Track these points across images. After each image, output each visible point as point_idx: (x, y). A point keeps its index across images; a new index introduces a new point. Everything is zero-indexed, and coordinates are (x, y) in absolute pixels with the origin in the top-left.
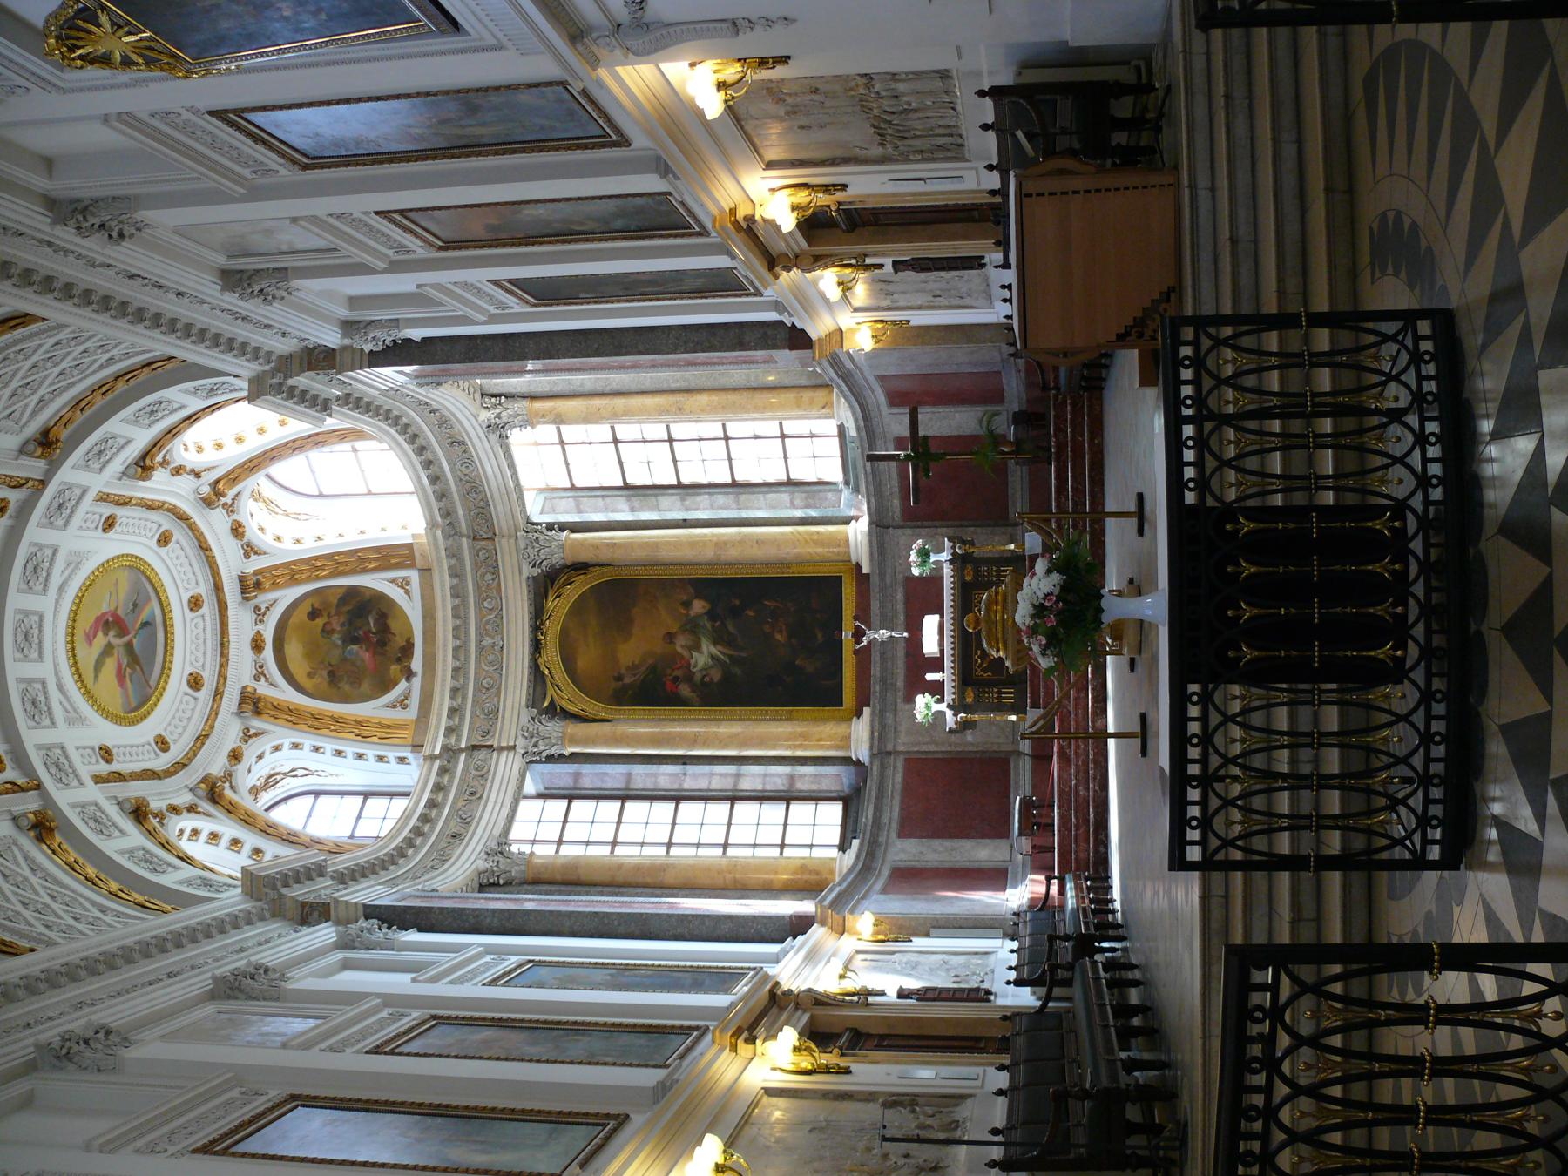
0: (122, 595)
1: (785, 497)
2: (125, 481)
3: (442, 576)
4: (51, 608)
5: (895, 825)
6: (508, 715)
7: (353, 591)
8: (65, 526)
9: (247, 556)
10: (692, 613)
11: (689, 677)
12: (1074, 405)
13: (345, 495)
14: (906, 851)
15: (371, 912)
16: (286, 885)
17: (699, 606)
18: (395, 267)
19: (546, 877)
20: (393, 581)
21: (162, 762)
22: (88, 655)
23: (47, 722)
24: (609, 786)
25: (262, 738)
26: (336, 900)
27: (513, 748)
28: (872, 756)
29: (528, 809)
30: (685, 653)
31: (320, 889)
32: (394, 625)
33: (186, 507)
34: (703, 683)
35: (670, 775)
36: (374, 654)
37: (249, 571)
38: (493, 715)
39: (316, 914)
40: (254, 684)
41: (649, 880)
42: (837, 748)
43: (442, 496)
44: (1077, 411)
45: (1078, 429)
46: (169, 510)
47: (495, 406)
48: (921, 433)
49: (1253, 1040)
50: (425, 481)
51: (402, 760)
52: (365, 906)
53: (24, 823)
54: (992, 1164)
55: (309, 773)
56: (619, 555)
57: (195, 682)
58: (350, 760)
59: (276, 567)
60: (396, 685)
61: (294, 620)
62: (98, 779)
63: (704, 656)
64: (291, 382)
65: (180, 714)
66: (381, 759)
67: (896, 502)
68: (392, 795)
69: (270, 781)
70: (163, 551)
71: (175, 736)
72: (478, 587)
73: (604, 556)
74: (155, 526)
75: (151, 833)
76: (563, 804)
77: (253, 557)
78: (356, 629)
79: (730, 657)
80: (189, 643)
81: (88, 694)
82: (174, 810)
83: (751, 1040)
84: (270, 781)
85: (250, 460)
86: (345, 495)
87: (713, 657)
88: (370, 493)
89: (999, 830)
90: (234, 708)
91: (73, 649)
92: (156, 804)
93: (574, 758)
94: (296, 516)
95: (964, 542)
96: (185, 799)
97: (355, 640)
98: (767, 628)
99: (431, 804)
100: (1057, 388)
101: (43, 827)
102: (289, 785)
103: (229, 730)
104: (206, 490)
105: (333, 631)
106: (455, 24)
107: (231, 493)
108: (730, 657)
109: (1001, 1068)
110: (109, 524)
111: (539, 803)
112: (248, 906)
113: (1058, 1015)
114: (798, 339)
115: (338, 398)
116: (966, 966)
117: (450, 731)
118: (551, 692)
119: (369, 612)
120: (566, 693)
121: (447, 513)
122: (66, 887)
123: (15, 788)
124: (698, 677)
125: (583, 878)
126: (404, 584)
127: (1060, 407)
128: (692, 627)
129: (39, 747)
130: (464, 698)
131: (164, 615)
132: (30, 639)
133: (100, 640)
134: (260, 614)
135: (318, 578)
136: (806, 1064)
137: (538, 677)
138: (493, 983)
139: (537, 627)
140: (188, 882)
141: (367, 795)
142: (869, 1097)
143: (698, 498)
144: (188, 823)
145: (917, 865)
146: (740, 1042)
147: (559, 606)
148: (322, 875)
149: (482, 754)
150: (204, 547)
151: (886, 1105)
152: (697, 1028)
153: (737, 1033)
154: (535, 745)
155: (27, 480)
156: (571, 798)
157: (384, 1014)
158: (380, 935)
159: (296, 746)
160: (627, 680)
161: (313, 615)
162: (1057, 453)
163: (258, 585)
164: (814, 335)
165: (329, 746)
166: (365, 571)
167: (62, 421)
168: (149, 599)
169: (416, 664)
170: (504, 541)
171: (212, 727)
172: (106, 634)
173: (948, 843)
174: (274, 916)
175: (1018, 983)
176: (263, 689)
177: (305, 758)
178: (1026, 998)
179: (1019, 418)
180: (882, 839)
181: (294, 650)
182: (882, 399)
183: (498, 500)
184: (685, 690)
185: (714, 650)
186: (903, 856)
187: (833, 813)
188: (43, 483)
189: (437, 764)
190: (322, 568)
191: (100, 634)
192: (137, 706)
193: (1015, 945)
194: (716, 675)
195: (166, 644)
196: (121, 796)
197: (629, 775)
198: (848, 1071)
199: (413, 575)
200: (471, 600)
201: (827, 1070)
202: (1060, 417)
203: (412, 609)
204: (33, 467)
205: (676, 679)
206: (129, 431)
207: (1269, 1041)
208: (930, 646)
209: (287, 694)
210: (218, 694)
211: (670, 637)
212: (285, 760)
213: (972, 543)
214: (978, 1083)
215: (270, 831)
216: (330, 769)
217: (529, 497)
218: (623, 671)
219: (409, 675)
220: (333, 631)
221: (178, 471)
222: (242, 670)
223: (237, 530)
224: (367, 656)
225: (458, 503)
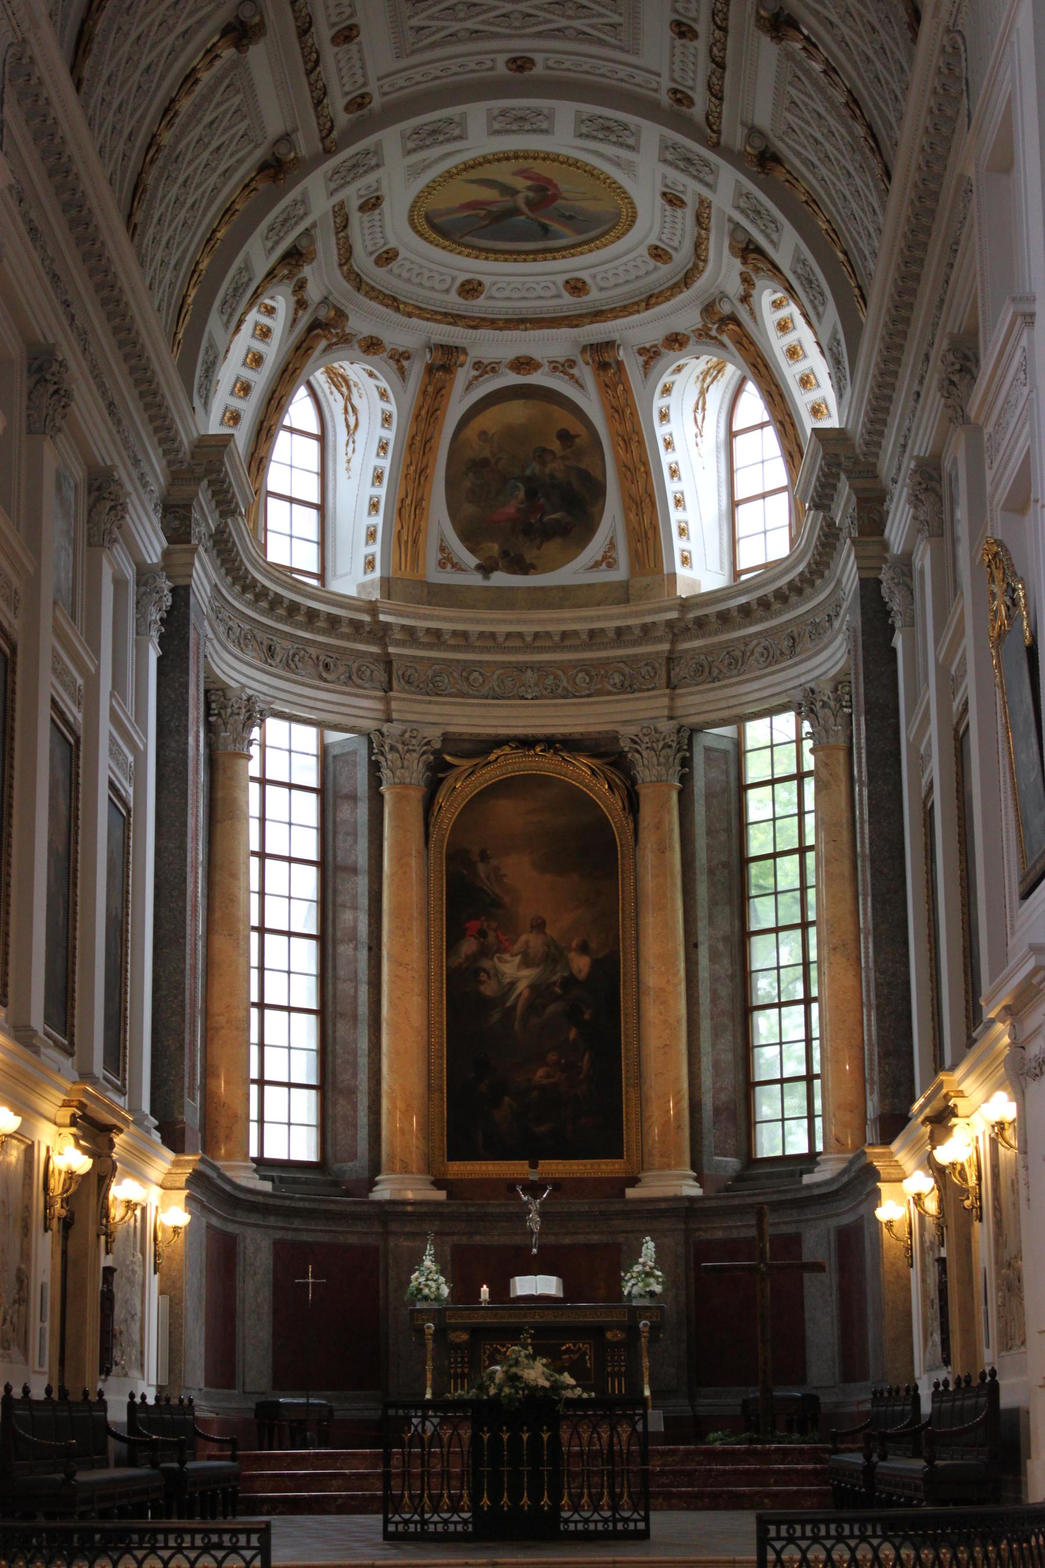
0: (584, 204)
1: (729, 1080)
2: (728, 227)
3: (619, 617)
4: (562, 134)
5: (290, 1236)
6: (436, 709)
7: (599, 490)
8: (665, 161)
9: (642, 351)
10: (572, 955)
11: (485, 952)
12: (815, 1473)
14: (257, 1250)
15: (181, 594)
16: (210, 483)
17: (581, 964)
18: (942, 670)
19: (220, 777)
20: (612, 546)
21: (363, 261)
22: (502, 173)
23: (410, 145)
24: (340, 844)
25: (397, 381)
26: (194, 550)
27: (389, 720)
28: (380, 1204)
29: (307, 738)
30: (517, 947)
31: (205, 519)
32: (552, 547)
33: (701, 282)
34: (477, 972)
35: (355, 928)
37: (622, 355)
38: (432, 688)
39: (176, 524)
40: (469, 361)
41: (218, 915)
42: (392, 1157)
43: (724, 618)
44: (804, 1476)
45: (785, 1477)
46: (695, 266)
47: (838, 700)
48: (806, 1276)
49: (220, 1538)
50: (743, 600)
51: (370, 564)
52: (187, 588)
53: (282, 149)
54: (8, 1388)
55: (352, 431)
56: (648, 857)
57: (470, 289)
58: (371, 491)
59: (627, 391)
60: (472, 551)
61: (558, 412)
62: (341, 213)
63: (514, 973)
64: (843, 477)
65: (427, 274)
66: (371, 535)
67: (720, 1234)
68: (322, 544)
69: (340, 381)
70: (643, 250)
71: (396, 271)
72: (606, 662)
73: (648, 839)
74: (676, 244)
75: (270, 275)
76: (313, 782)
77: (641, 359)
79: (514, 1007)
81: (449, 175)
82: (301, 286)
83: (73, 1123)
84: (340, 381)
85: (766, 366)
87: (513, 984)
88: (734, 504)
89: (282, 1380)
90: (436, 339)
91: (508, 159)
92: (307, 271)
93: (376, 800)
94: (700, 405)
95: (654, 1329)
96: (314, 293)
97: (531, 494)
98: (552, 1057)
99: (312, 615)
100: (837, 1451)
101: (277, 169)
102: (335, 404)
103: (407, 334)
104: (726, 309)
105: (543, 463)
106: (1025, 895)
107: (725, 339)
108: (514, 1007)
109: (49, 1391)
110: (673, 200)
111: (313, 747)
112: (186, 442)
113: (104, 1451)
114: (892, 1125)
115: (830, 523)
116: (130, 1342)
117: (410, 631)
118: (466, 764)
120: (462, 786)
121: (701, 623)
122: (204, 215)
123: (327, 129)
124: (486, 964)
125: (219, 827)
126: (608, 561)
127: (813, 1456)
128: (553, 956)
129: (379, 144)
130: (455, 648)
131: (558, 250)
132: (521, 122)
134: (564, 367)
135: (614, 445)
136: (57, 1185)
137: (483, 747)
138: (112, 785)
139: (552, 743)
140: (211, 346)
141: (321, 508)
142: (26, 1255)
143: (726, 961)
144: (281, 302)
145: (239, 1269)
146: (70, 1111)
147: (580, 771)
148: (223, 515)
149: (381, 676)
150: (650, 301)
151: (19, 1270)
152: (72, 1043)
153: (82, 1106)
154: (392, 748)
155: (718, 132)
156: (321, 792)
157: (80, 681)
158: (155, 616)
159: (387, 419)
160: (481, 868)
161: (565, 436)
162: (755, 1452)
163: (603, 366)
164: (894, 1146)
165: (386, 464)
166: (626, 509)
167: (793, 179)
168: (579, 232)
169: (501, 579)
170: (665, 701)
171: (410, 315)
172: (529, 188)
173: (266, 1309)
174: (172, 472)
175: (132, 1407)
176: (463, 375)
177: (372, 431)
178: (117, 1414)
179: (811, 1401)
180: (272, 1221)
181: (516, 412)
182: (846, 1220)
183: (721, 694)
184: (469, 946)
185: (522, 986)
186: (251, 1249)
187: (303, 1147)
188: (715, 147)
189: (367, 618)
190: (627, 449)
191: (529, 183)
192: (440, 227)
193: (151, 1401)
194: (489, 989)
195: (519, 253)
196: (317, 232)
197: (354, 870)
198: (46, 1230)
199: (620, 574)
200: (587, 655)
201: (48, 1205)
202: (802, 1455)
203: (573, 572)
204: (734, 137)
205: (483, 934)
206: (787, 247)
207: (219, 1546)
208: (525, 1285)
209: (458, 404)
210: (453, 319)
211: (539, 926)
213: (653, 1340)
214: (37, 1368)
215: (275, 404)
216: (357, 460)
217: (728, 731)
218: (494, 862)
219: (485, 569)
220: (543, 463)
221: (746, 280)
223: (676, 341)
224: (510, 510)
225: (716, 639)
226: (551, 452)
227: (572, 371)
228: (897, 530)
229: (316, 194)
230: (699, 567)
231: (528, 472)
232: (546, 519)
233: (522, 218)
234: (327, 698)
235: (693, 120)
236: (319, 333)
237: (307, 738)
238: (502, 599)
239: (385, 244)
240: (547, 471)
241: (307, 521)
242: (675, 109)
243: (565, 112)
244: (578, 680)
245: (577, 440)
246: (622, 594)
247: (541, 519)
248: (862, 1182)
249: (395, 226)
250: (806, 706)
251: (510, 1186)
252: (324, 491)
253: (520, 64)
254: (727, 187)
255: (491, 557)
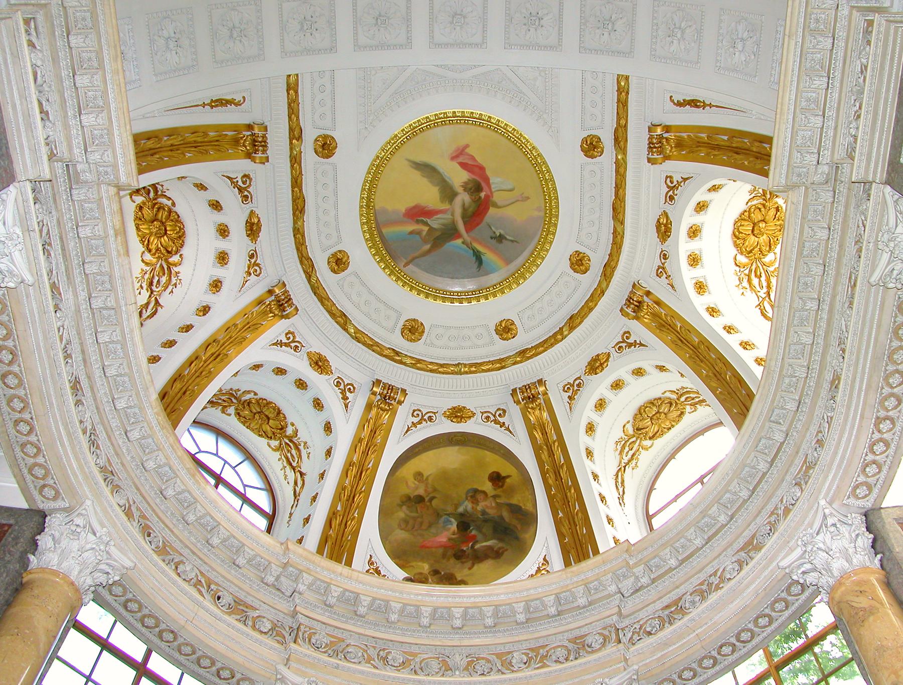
36: (445, 547)
60: (401, 567)
61: (489, 456)
78: (479, 529)
80: (459, 322)
97: (464, 526)
119: (501, 540)
133: (458, 177)
134: (496, 417)
161: (497, 479)
172: (465, 187)
176: (403, 416)
181: (451, 458)
210: (395, 356)
222: (427, 394)
226: (484, 492)
227: (501, 420)
231: (461, 509)
232: (477, 546)
233: (459, 242)
239: (338, 243)
240: (479, 508)
244: (514, 661)
245: (508, 480)
247: (472, 547)
255: (421, 574)
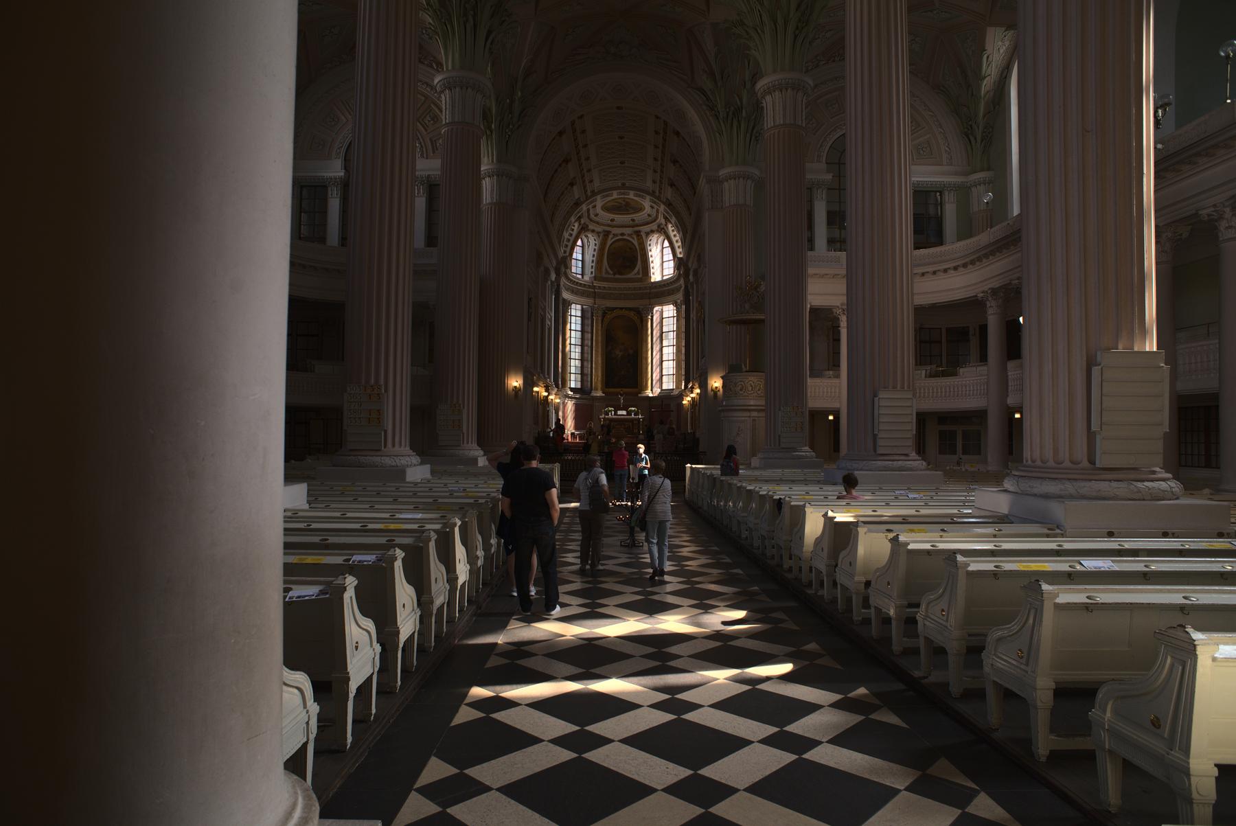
13: (661, 262)
15: (559, 285)
17: (631, 352)
21: (592, 216)
31: (563, 269)
38: (603, 297)
57: (612, 220)
63: (619, 353)
86: (661, 262)
101: (577, 204)
103: (599, 229)
137: (613, 309)
147: (632, 314)
150: (648, 223)
177: (592, 246)
192: (605, 208)
203: (631, 275)
206: (673, 220)
208: (620, 412)
209: (609, 243)
212: (592, 242)
223: (652, 231)
228: (691, 277)
229: (584, 207)
230: (656, 277)
234: (583, 300)
235: (656, 197)
236: (584, 229)
237: (579, 307)
238: (616, 281)
241: (580, 264)
242: (652, 194)
243: (632, 193)
246: (640, 280)
248: (681, 396)
249: (599, 210)
250: (675, 304)
251: (617, 394)
252: (581, 257)
253: (623, 184)
254: (662, 207)
